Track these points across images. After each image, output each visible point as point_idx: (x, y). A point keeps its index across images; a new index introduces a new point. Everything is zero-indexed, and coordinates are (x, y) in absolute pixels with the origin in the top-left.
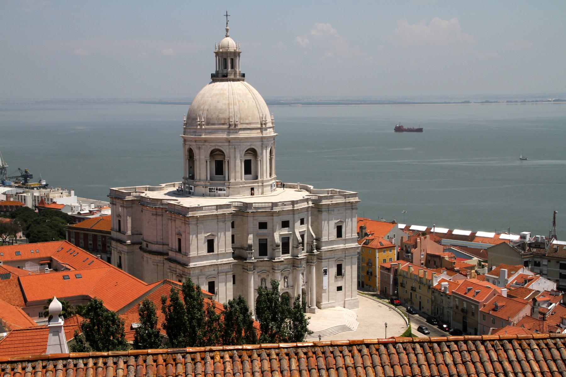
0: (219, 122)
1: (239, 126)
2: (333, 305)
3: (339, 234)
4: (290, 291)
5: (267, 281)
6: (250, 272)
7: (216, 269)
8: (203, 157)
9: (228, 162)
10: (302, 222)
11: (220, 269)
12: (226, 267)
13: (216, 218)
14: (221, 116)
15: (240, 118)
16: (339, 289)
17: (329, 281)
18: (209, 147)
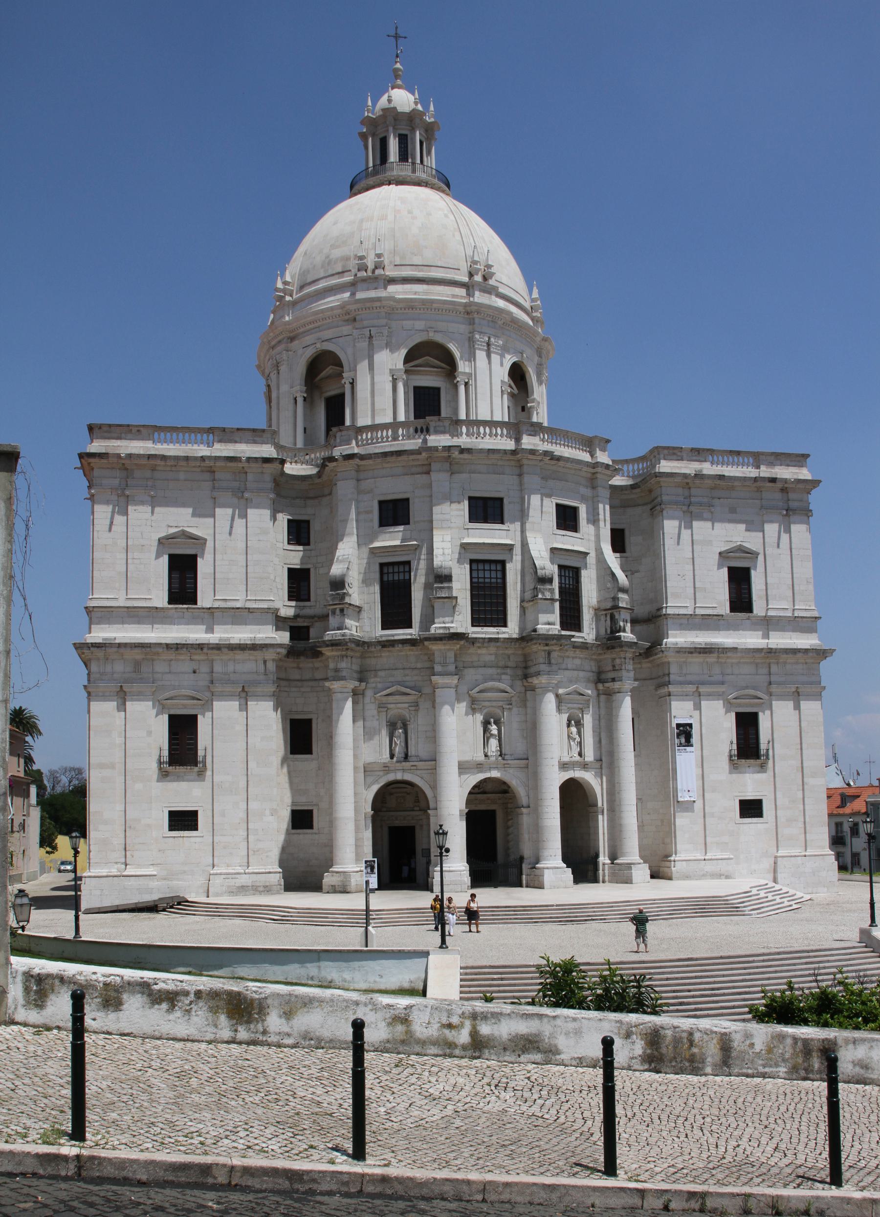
0: (330, 272)
1: (390, 272)
2: (723, 867)
3: (741, 598)
4: (515, 780)
5: (411, 727)
6: (336, 685)
7: (204, 668)
8: (284, 388)
9: (352, 384)
10: (567, 519)
11: (218, 668)
12: (248, 665)
13: (207, 476)
14: (337, 253)
15: (394, 252)
16: (751, 808)
17: (704, 770)
18: (300, 351)
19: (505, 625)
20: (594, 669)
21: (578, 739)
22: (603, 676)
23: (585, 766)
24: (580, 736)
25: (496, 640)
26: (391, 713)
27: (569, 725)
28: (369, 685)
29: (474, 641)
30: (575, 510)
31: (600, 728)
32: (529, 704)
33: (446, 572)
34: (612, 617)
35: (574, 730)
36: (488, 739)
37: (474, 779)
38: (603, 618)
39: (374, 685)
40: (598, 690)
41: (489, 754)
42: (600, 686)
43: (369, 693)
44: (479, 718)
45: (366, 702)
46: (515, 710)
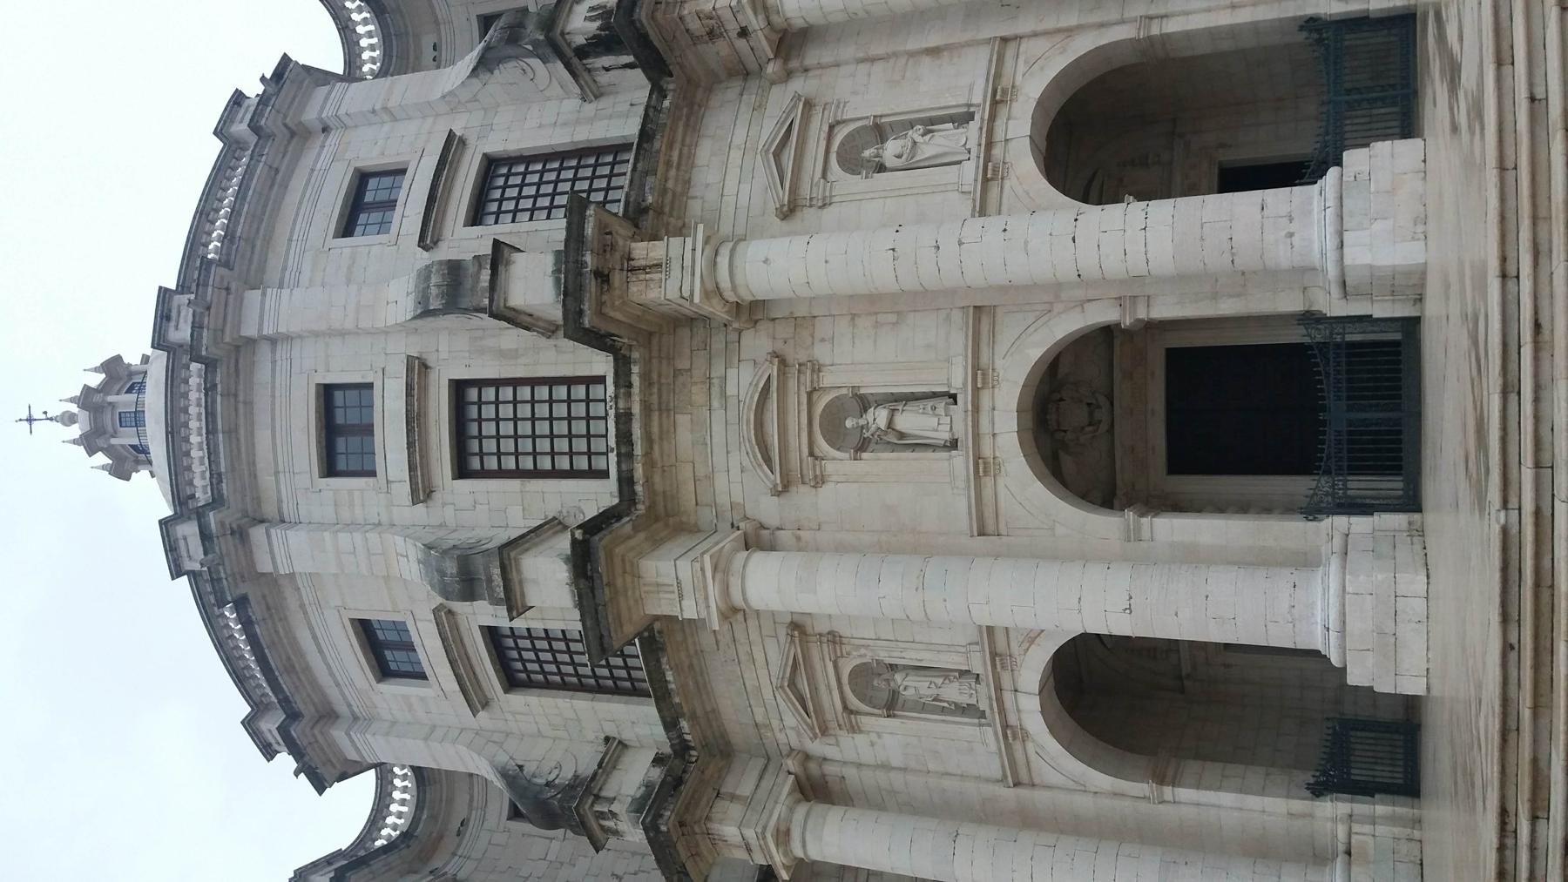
19: (601, 380)
20: (732, 94)
21: (915, 134)
22: (752, 64)
23: (998, 100)
24: (911, 124)
25: (624, 419)
26: (854, 702)
27: (881, 168)
28: (795, 743)
29: (626, 481)
30: (362, 178)
31: (895, 55)
32: (801, 311)
33: (451, 567)
34: (582, 52)
35: (892, 148)
36: (902, 435)
37: (1022, 487)
38: (604, 78)
39: (793, 736)
40: (789, 75)
41: (947, 436)
42: (771, 69)
43: (817, 747)
44: (838, 463)
45: (838, 757)
46: (821, 353)
